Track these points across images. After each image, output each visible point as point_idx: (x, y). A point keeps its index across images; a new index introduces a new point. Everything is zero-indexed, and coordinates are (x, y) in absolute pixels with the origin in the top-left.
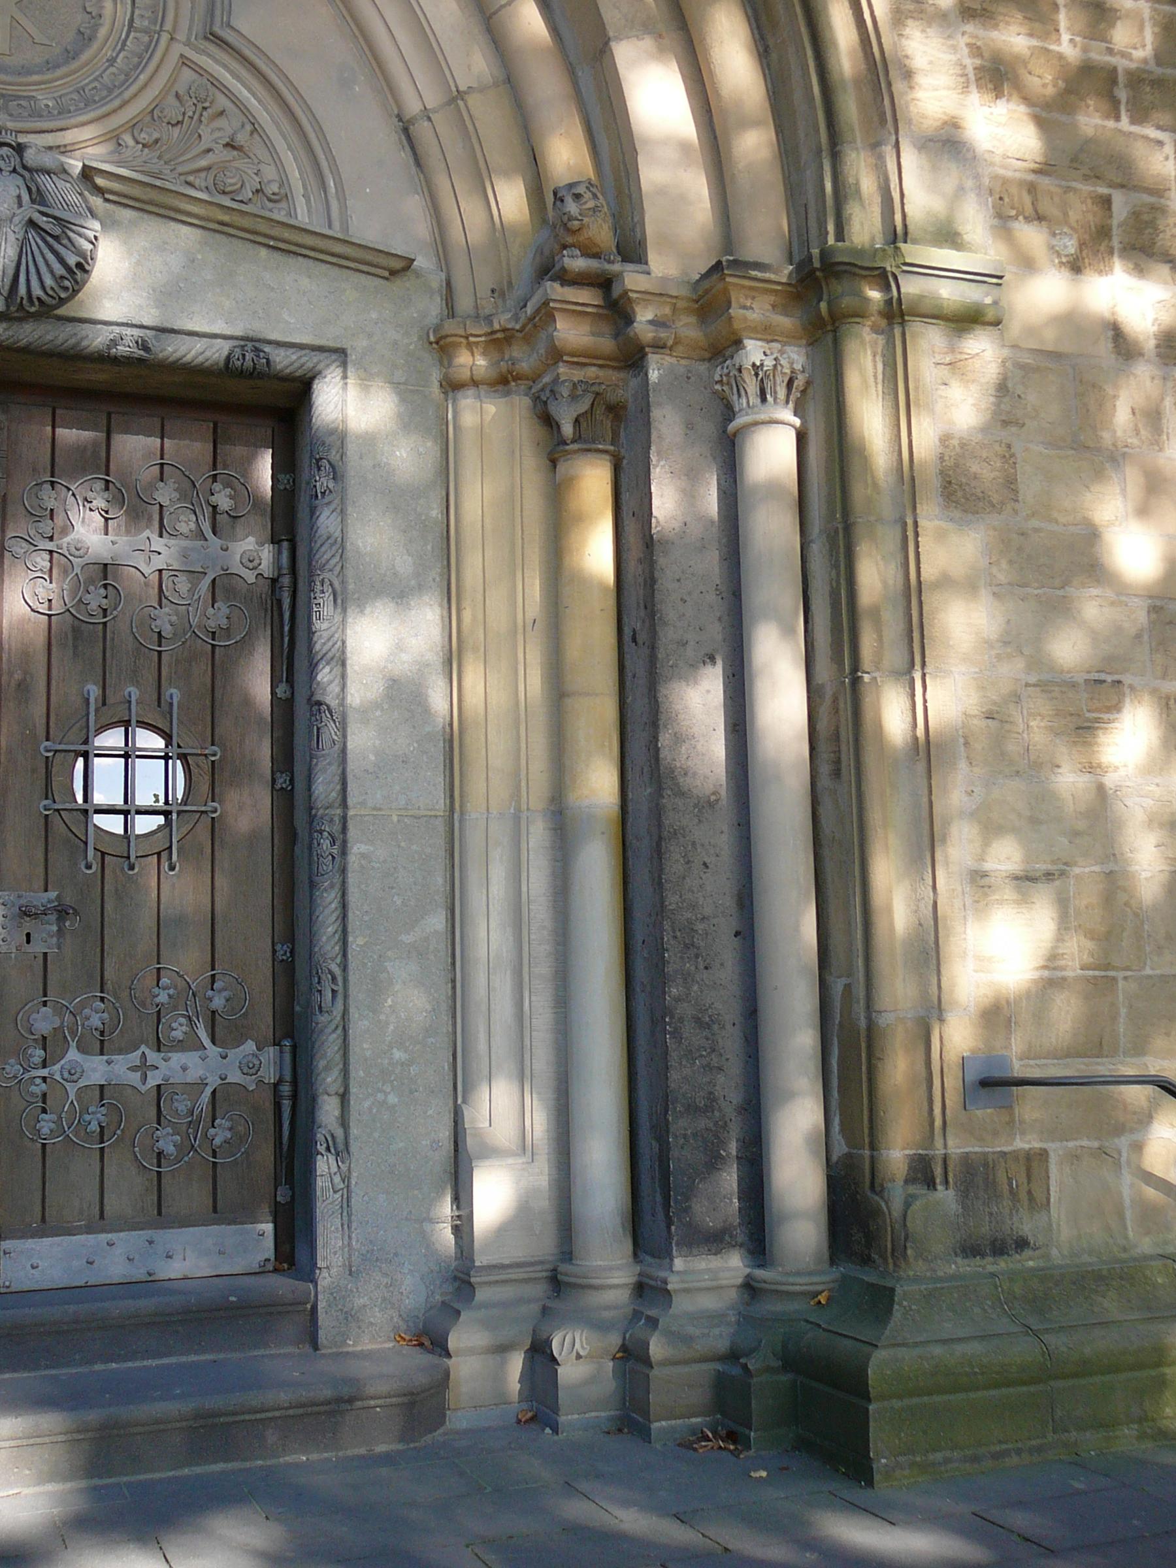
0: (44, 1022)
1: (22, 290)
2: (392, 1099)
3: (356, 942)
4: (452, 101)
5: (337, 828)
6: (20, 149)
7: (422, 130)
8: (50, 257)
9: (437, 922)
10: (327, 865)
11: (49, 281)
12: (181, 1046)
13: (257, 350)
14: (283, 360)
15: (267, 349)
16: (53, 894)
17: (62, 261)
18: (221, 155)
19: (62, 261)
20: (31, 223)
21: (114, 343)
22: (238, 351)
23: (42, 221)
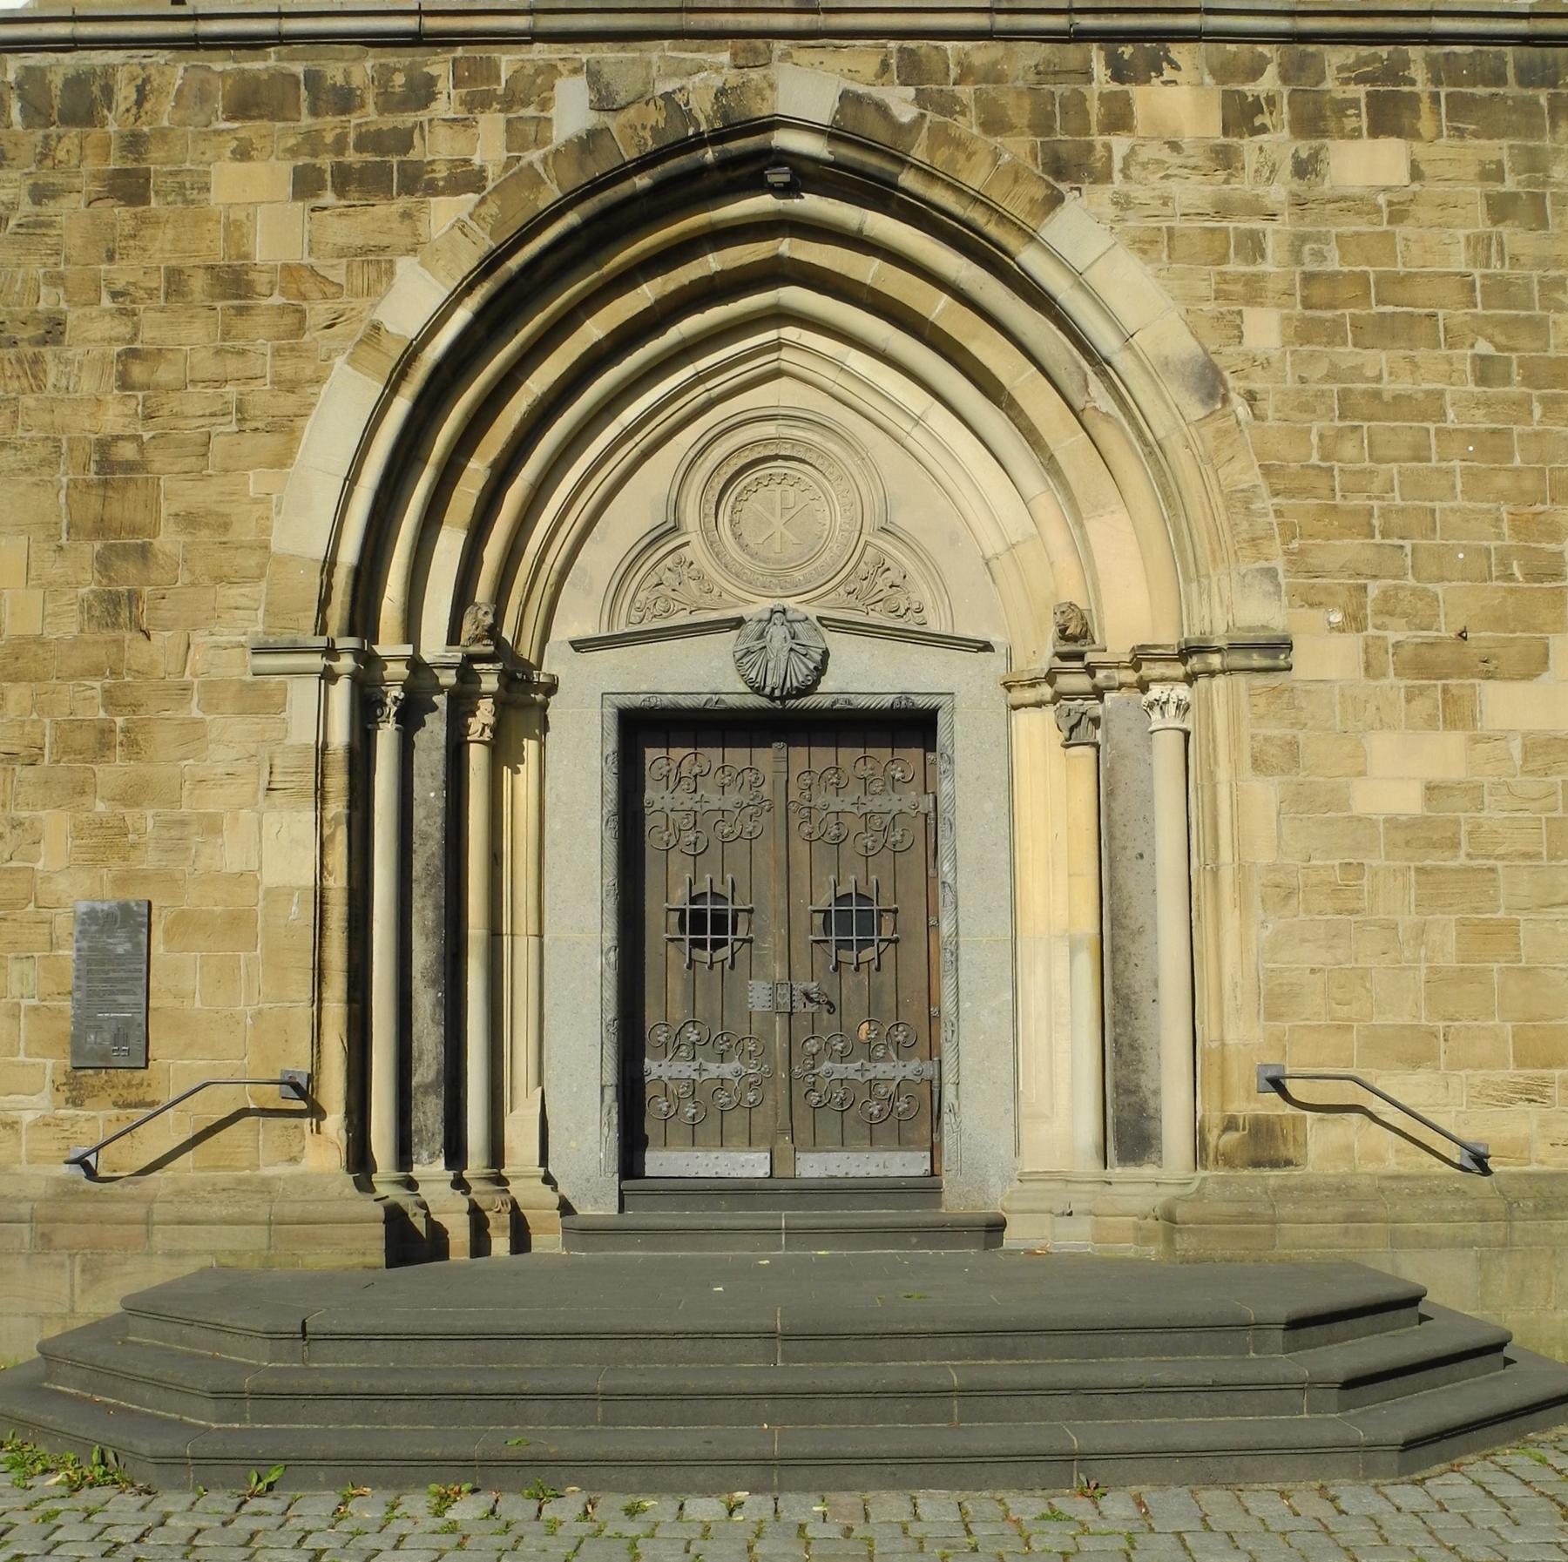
0: (813, 1046)
1: (788, 684)
2: (983, 1087)
3: (965, 1005)
4: (1008, 549)
5: (953, 949)
6: (784, 612)
7: (994, 564)
8: (801, 666)
9: (1009, 996)
10: (948, 966)
11: (801, 679)
12: (879, 1059)
13: (907, 699)
14: (921, 702)
15: (913, 697)
16: (815, 984)
17: (807, 667)
18: (887, 592)
19: (807, 667)
20: (791, 650)
21: (834, 703)
22: (897, 701)
23: (797, 648)
